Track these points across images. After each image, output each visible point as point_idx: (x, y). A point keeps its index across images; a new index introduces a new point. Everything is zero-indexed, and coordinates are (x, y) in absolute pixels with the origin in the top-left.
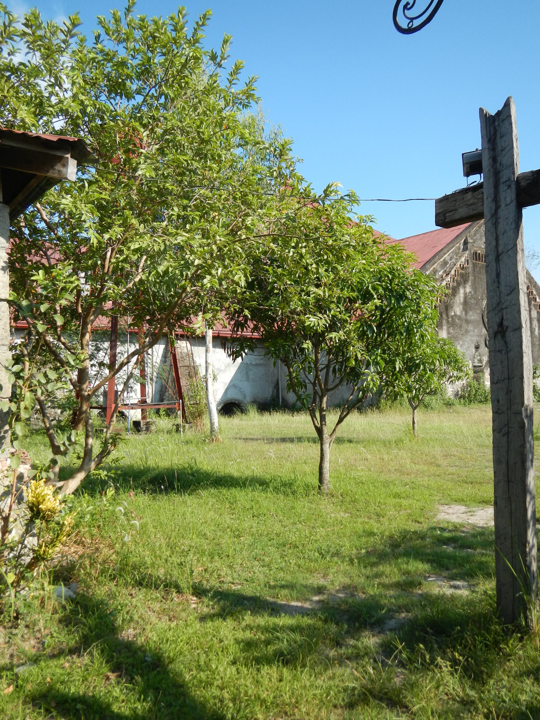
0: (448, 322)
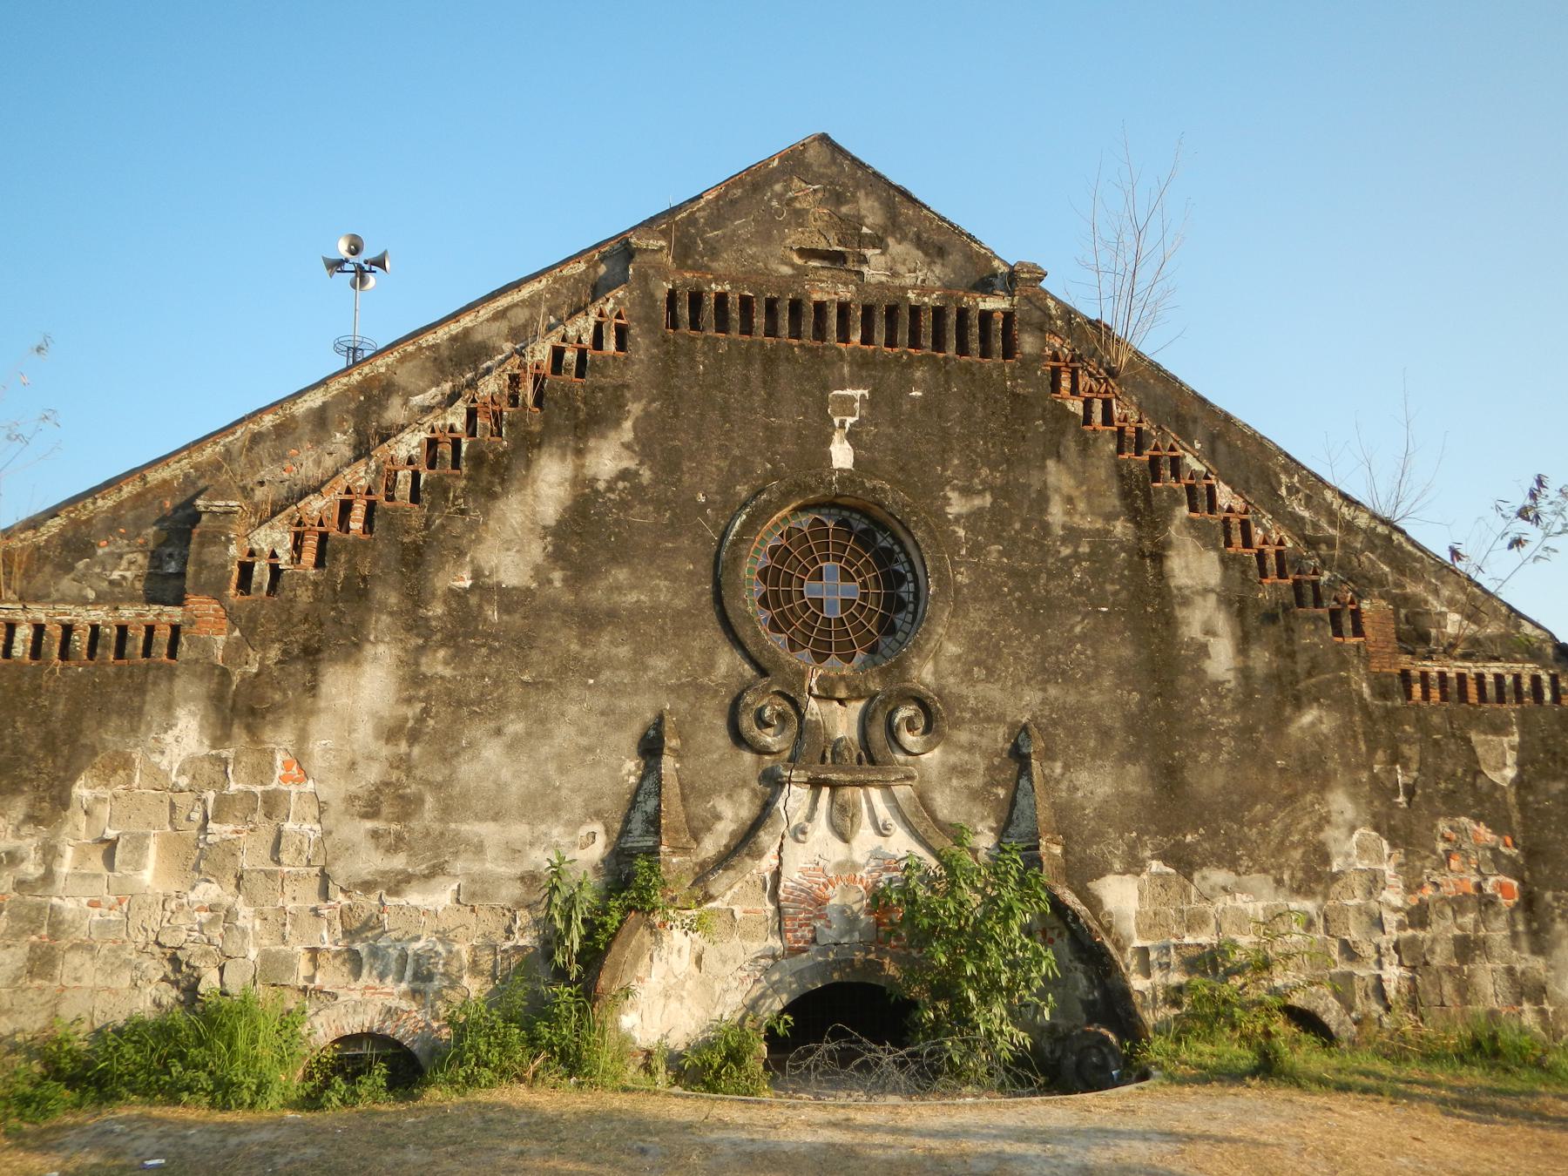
0: (413, 623)
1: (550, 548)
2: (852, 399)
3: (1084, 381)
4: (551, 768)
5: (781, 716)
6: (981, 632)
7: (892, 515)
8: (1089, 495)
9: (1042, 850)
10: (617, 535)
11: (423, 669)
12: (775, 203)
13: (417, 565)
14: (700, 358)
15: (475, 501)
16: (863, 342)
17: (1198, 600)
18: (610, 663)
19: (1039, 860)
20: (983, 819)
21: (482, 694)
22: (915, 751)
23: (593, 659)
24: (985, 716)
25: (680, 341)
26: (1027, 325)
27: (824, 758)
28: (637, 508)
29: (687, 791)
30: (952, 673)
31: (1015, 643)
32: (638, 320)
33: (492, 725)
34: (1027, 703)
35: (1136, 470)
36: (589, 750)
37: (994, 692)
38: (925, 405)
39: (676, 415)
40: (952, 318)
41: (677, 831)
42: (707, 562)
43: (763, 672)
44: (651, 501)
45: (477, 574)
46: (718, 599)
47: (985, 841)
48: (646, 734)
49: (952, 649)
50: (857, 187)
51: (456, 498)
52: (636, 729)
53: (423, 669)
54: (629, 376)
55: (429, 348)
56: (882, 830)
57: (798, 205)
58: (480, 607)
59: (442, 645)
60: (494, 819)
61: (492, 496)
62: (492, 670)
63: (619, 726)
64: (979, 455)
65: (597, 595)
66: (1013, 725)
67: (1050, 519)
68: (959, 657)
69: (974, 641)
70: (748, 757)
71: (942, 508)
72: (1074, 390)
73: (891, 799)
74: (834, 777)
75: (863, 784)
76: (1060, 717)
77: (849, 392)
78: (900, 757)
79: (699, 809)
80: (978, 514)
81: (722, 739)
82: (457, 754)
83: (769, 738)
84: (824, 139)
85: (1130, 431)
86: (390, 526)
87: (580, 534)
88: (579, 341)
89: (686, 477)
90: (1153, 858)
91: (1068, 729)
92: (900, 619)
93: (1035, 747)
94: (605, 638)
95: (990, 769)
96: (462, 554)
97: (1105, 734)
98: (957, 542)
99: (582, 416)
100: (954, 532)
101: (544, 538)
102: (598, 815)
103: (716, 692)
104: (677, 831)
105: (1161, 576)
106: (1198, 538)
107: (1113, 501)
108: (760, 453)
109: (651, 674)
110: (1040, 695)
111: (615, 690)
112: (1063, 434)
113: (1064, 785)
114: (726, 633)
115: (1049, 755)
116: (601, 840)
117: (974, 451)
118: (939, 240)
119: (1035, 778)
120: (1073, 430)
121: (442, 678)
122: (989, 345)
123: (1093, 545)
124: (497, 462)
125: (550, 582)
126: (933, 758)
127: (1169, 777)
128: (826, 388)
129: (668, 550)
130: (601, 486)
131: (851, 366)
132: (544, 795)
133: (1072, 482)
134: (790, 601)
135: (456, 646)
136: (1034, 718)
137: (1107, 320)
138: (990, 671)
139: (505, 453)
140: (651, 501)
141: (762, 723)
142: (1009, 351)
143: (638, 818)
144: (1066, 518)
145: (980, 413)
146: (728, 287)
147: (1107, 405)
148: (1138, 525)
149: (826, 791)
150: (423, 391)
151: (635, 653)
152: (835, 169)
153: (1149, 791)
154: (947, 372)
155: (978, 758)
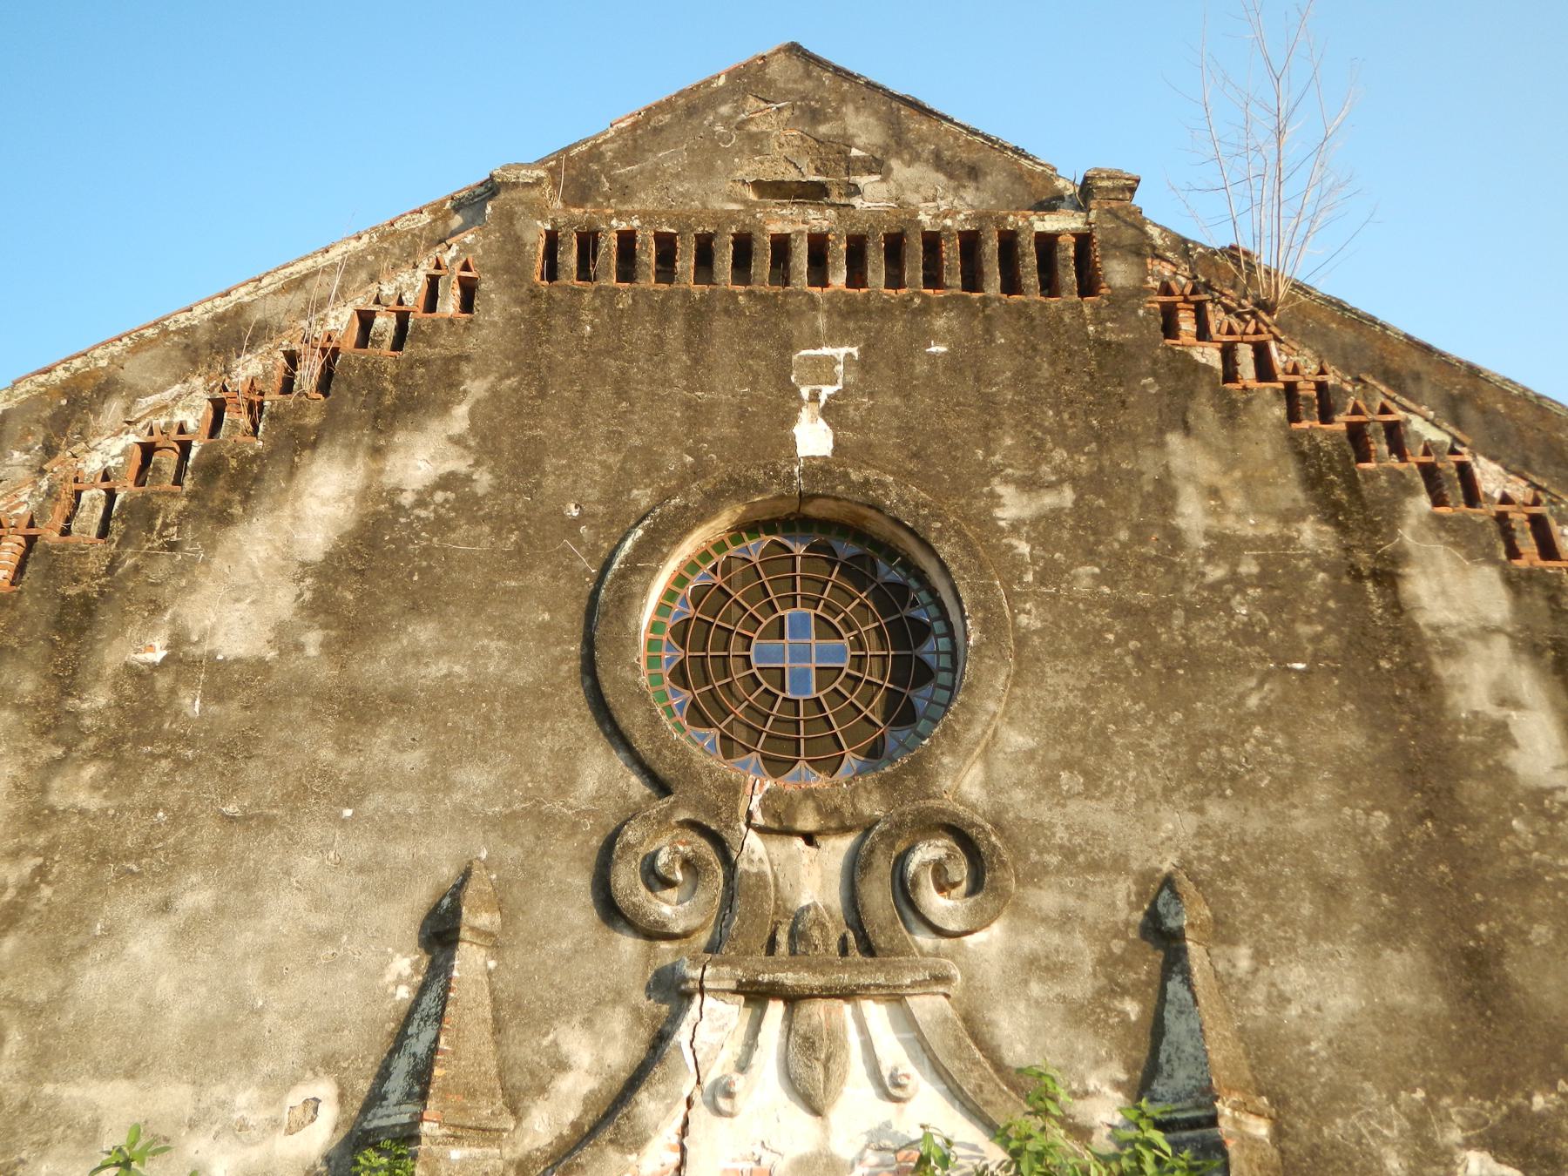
1: (308, 596)
2: (832, 361)
3: (1217, 319)
4: (251, 975)
5: (691, 865)
6: (1070, 710)
7: (897, 522)
8: (1248, 485)
9: (1225, 1126)
10: (422, 571)
11: (54, 798)
12: (719, 128)
13: (80, 630)
14: (587, 316)
15: (196, 529)
16: (849, 284)
17: (1475, 646)
18: (387, 780)
19: (1219, 1147)
20: (1098, 1063)
21: (147, 841)
22: (952, 926)
23: (359, 773)
24: (1086, 861)
25: (558, 295)
26: (1115, 247)
27: (772, 946)
28: (464, 529)
29: (505, 1014)
30: (1020, 783)
31: (1136, 727)
32: (494, 272)
33: (155, 894)
34: (1169, 835)
35: (1326, 445)
36: (328, 936)
37: (1101, 815)
38: (953, 364)
39: (542, 393)
40: (991, 246)
41: (471, 1093)
42: (576, 609)
43: (662, 787)
44: (488, 518)
45: (178, 640)
46: (589, 667)
47: (1106, 1110)
48: (438, 905)
49: (1017, 740)
50: (843, 100)
51: (165, 526)
52: (421, 896)
53: (54, 798)
54: (471, 345)
55: (179, 332)
56: (890, 1089)
57: (753, 128)
58: (173, 691)
59: (95, 756)
60: (130, 1075)
61: (224, 519)
62: (173, 797)
63: (388, 893)
64: (1047, 431)
65: (377, 667)
66: (1145, 877)
67: (1181, 523)
68: (1030, 755)
69: (1059, 725)
70: (628, 945)
71: (988, 510)
72: (1203, 334)
73: (908, 1023)
74: (788, 978)
75: (848, 994)
76: (1237, 861)
77: (826, 351)
78: (925, 940)
79: (526, 1049)
80: (1053, 517)
81: (581, 912)
82: (82, 949)
83: (667, 908)
84: (794, 49)
85: (1306, 388)
86: (51, 572)
87: (361, 573)
88: (400, 302)
89: (549, 482)
90: (1468, 1144)
91: (1254, 883)
92: (920, 698)
93: (1191, 915)
94: (384, 736)
95: (1106, 961)
96: (156, 608)
97: (1331, 891)
98: (1017, 564)
99: (388, 400)
100: (1011, 547)
101: (302, 579)
102: (329, 1063)
103: (575, 825)
104: (471, 1093)
105: (1397, 607)
106: (1456, 545)
107: (1290, 491)
108: (677, 442)
109: (458, 797)
110: (1190, 822)
111: (390, 828)
112: (1191, 394)
113: (1259, 994)
114: (601, 724)
115: (1221, 932)
116: (329, 1114)
117: (1040, 426)
118: (969, 156)
119: (1197, 978)
120: (1207, 389)
121: (82, 812)
122: (1054, 287)
123: (1264, 562)
124: (242, 471)
125: (299, 647)
126: (990, 941)
127: (1475, 975)
128: (788, 346)
129: (507, 591)
130: (407, 499)
131: (829, 313)
132: (231, 1025)
133: (1215, 466)
134: (727, 673)
135: (119, 759)
136: (1185, 863)
137: (1245, 244)
138: (1093, 779)
139: (257, 456)
140: (488, 518)
141: (656, 880)
142: (1088, 283)
143: (402, 1065)
144: (1211, 521)
145: (1046, 371)
146: (636, 223)
147: (1261, 352)
148: (1343, 529)
149: (776, 1009)
150: (162, 389)
151: (434, 759)
152: (809, 84)
153: (1437, 1003)
154: (988, 318)
155: (1079, 941)
